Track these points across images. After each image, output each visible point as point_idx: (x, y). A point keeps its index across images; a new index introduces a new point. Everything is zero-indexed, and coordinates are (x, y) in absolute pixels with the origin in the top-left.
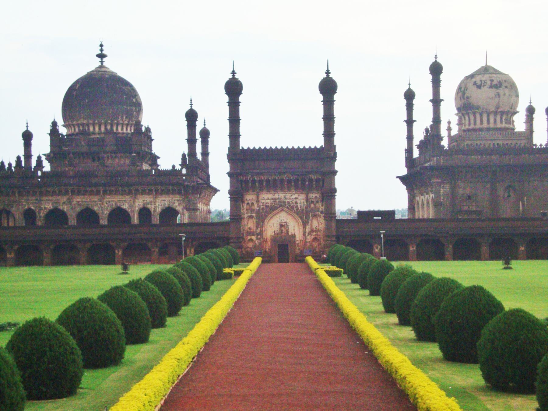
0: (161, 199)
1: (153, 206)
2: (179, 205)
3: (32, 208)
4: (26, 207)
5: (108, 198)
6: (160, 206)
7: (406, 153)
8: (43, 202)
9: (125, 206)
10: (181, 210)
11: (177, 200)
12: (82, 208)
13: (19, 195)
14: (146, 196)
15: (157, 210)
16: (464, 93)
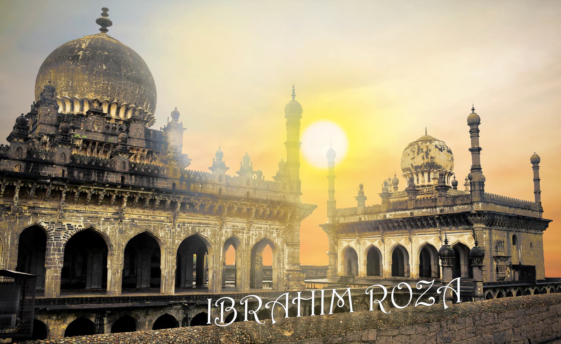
0: (256, 226)
1: (245, 236)
2: (278, 236)
3: (43, 224)
4: (30, 223)
5: (183, 218)
6: (254, 237)
7: (328, 204)
8: (67, 214)
9: (207, 234)
10: (279, 244)
11: (277, 229)
12: (139, 231)
13: (21, 197)
14: (238, 219)
15: (251, 242)
16: (427, 154)
